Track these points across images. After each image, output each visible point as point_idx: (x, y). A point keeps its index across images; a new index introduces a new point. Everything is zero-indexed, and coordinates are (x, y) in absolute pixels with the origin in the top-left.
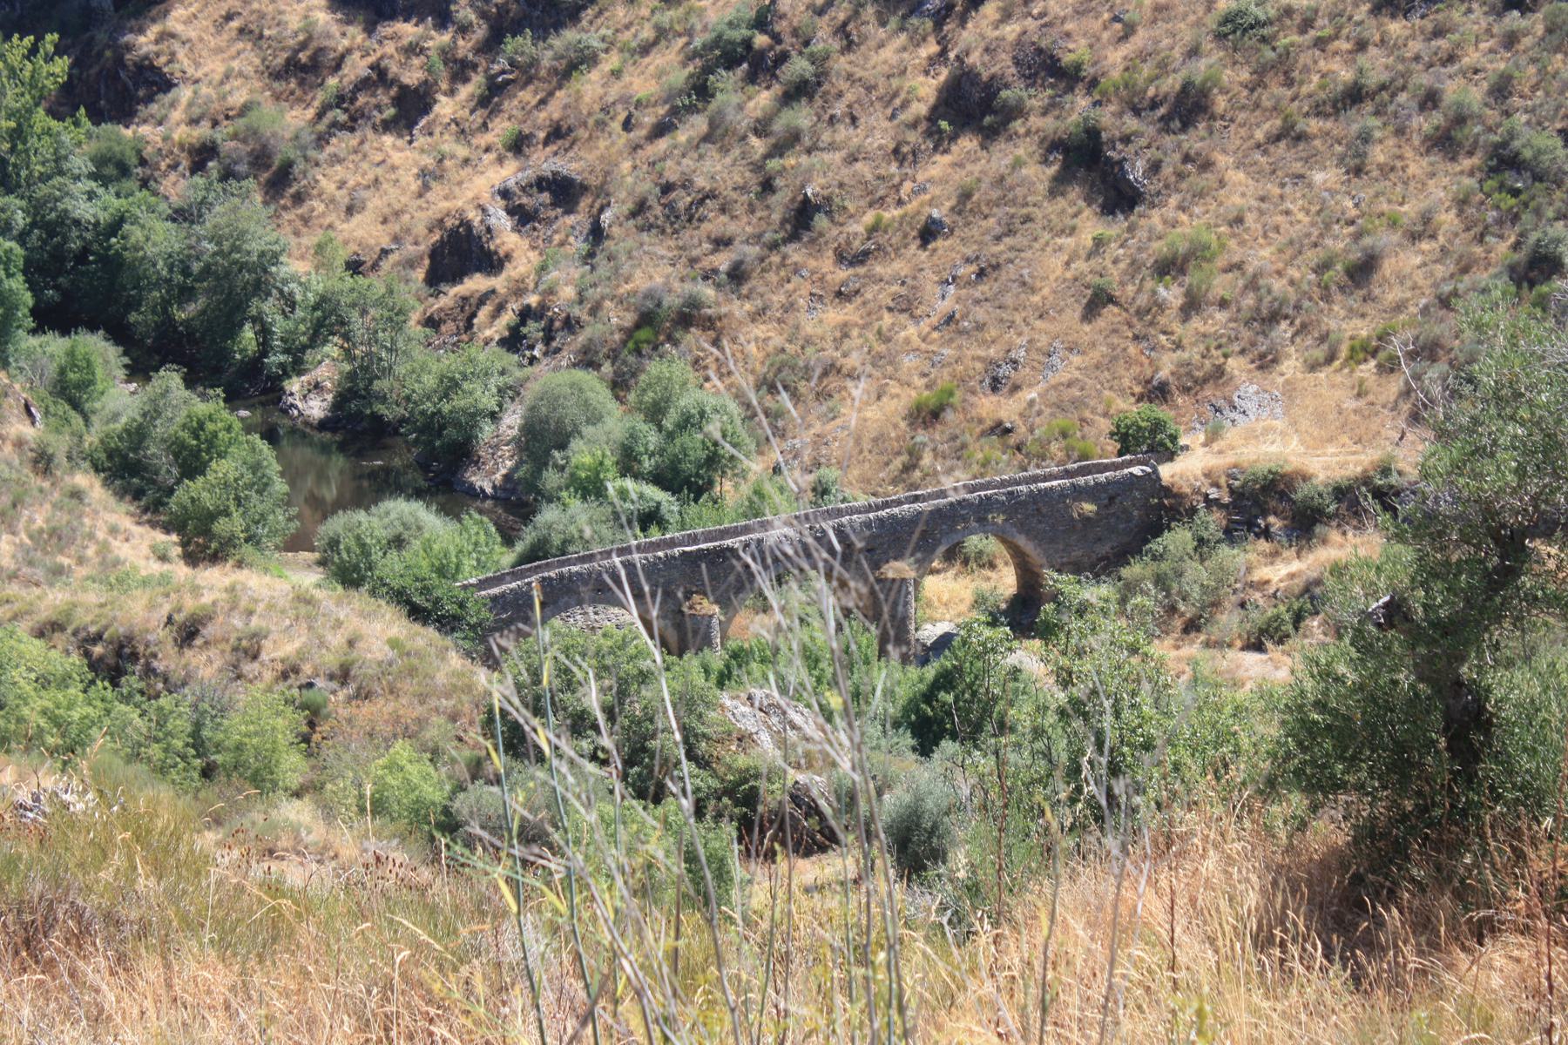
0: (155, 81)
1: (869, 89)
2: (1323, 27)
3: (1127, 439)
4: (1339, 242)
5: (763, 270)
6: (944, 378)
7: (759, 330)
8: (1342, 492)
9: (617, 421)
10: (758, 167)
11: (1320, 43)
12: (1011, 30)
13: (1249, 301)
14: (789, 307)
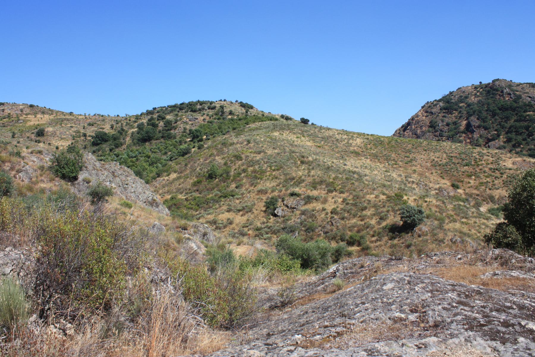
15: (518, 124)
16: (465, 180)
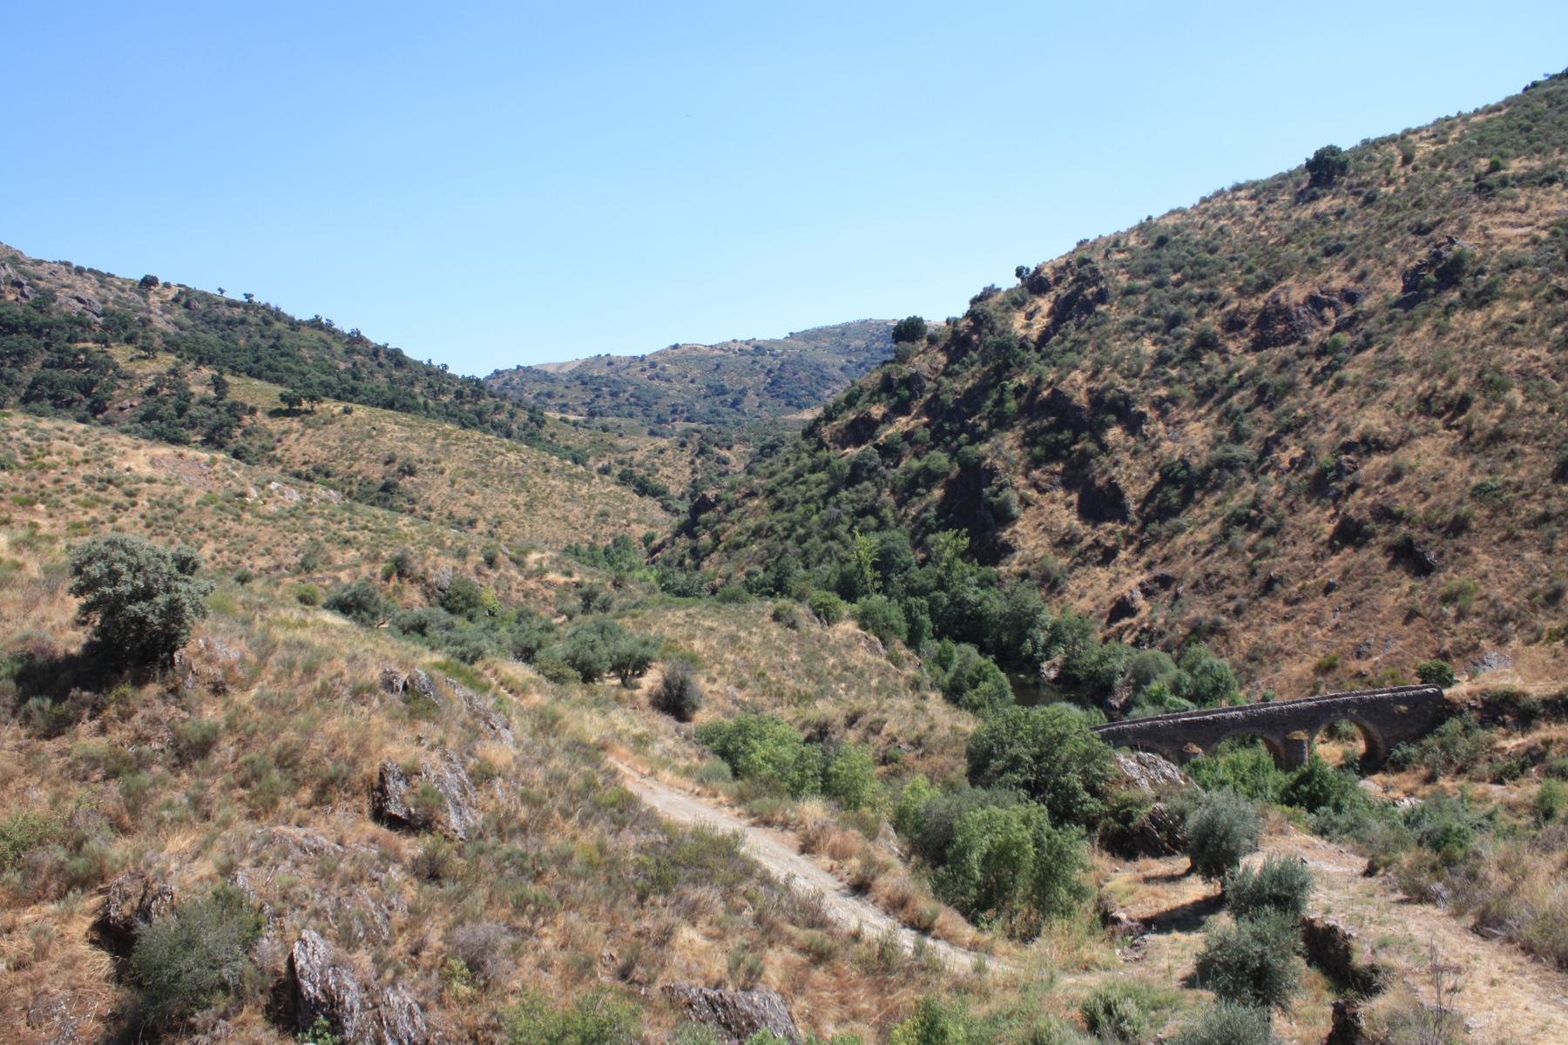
0: (1008, 549)
1: (1302, 529)
2: (1527, 489)
3: (1425, 675)
4: (1541, 584)
6: (1333, 652)
7: (1247, 635)
8: (1546, 702)
9: (1173, 671)
10: (1249, 565)
11: (1526, 497)
12: (1369, 500)
13: (1492, 612)
14: (1261, 624)
15: (60, 375)
16: (15, 516)
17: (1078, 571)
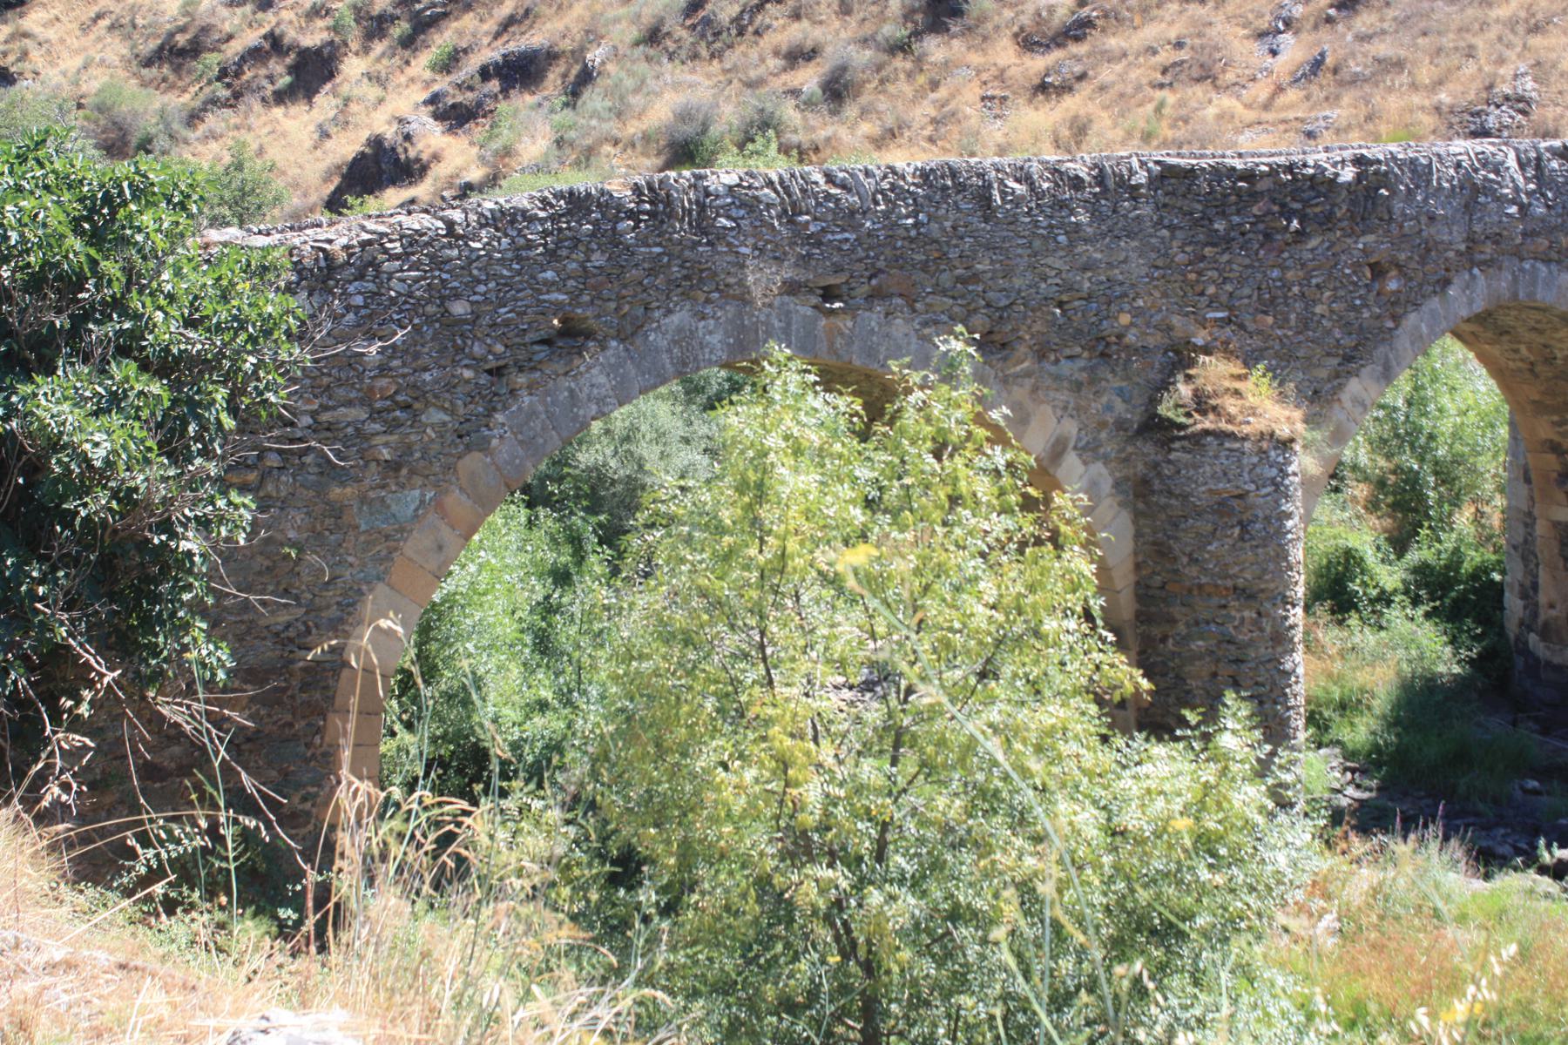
5: (882, 82)
17: (212, 121)
